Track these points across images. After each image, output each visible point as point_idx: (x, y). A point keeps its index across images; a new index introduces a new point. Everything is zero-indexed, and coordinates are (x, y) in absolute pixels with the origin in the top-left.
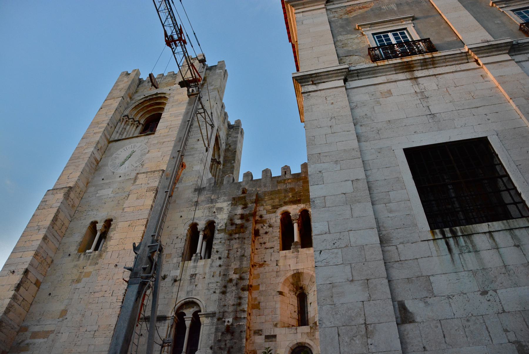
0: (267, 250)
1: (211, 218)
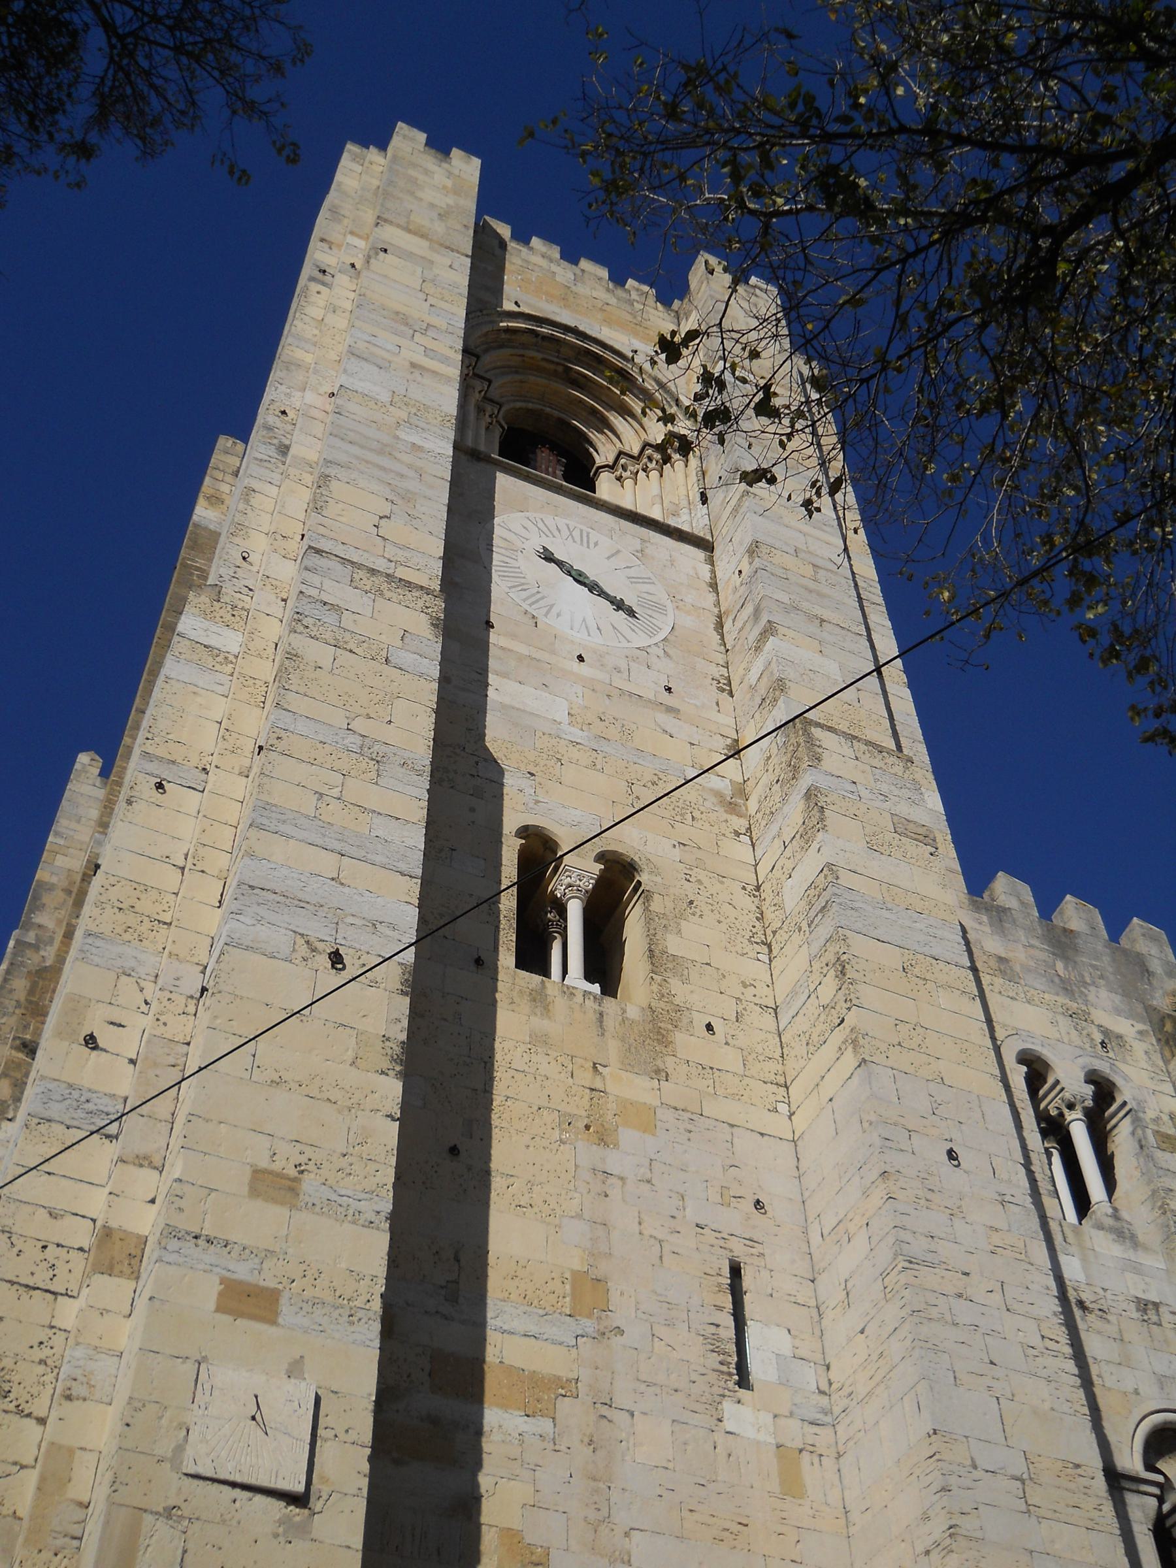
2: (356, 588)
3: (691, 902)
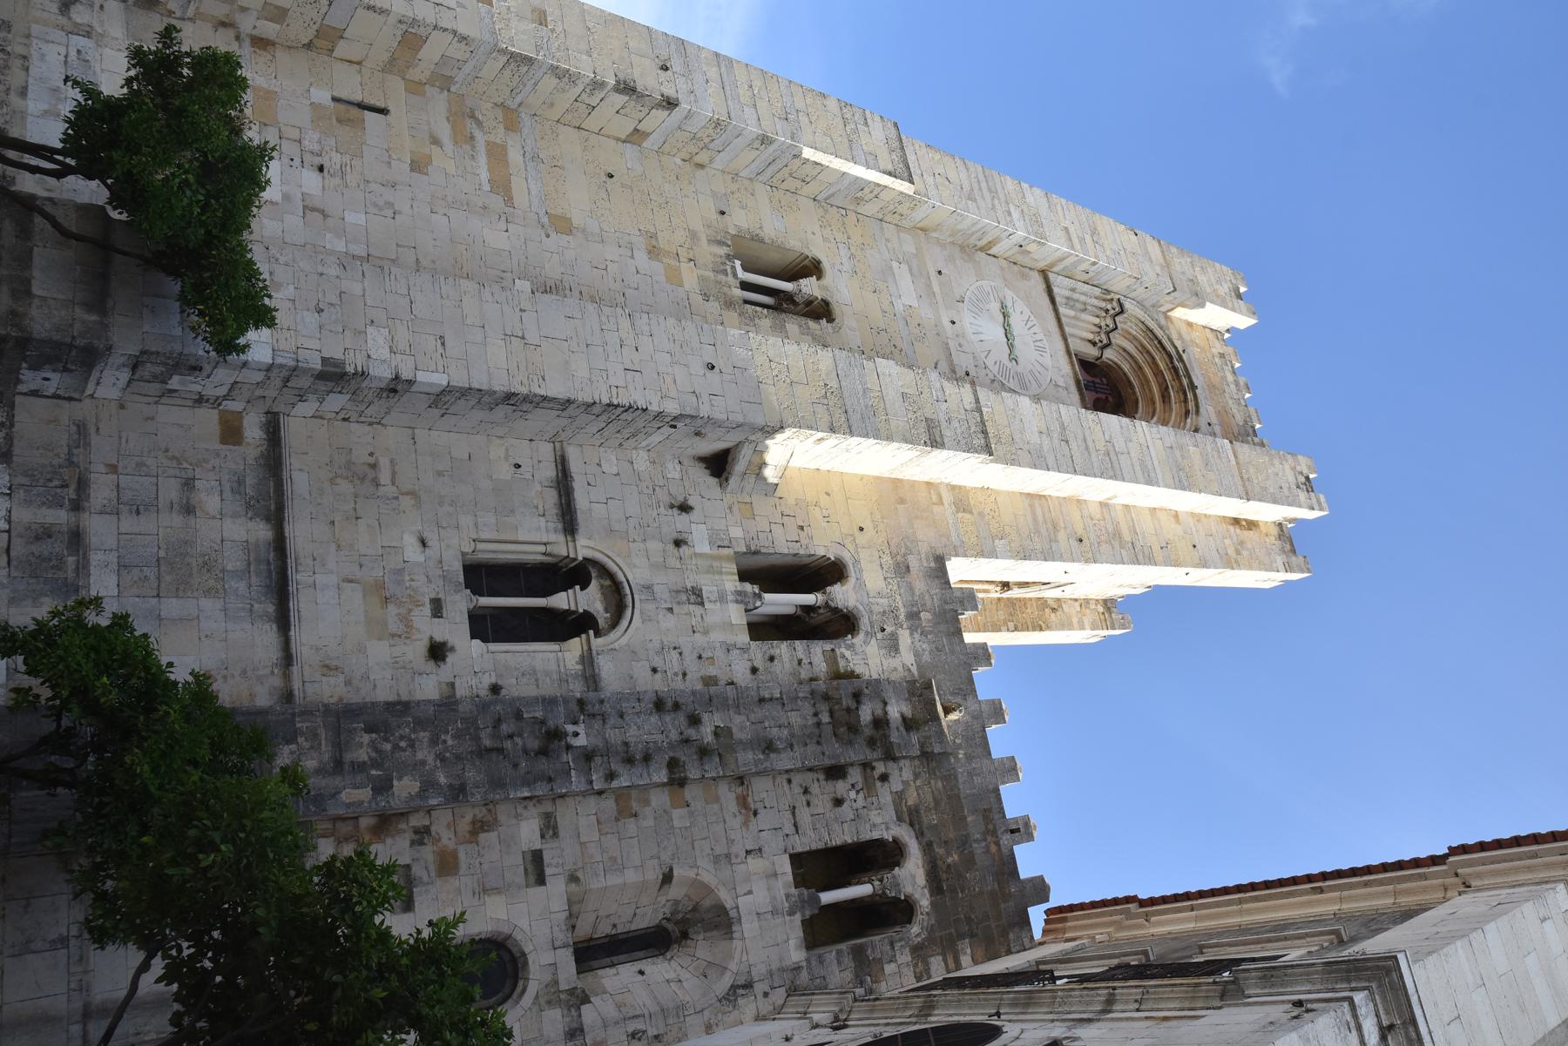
0: (788, 815)
1: (864, 623)
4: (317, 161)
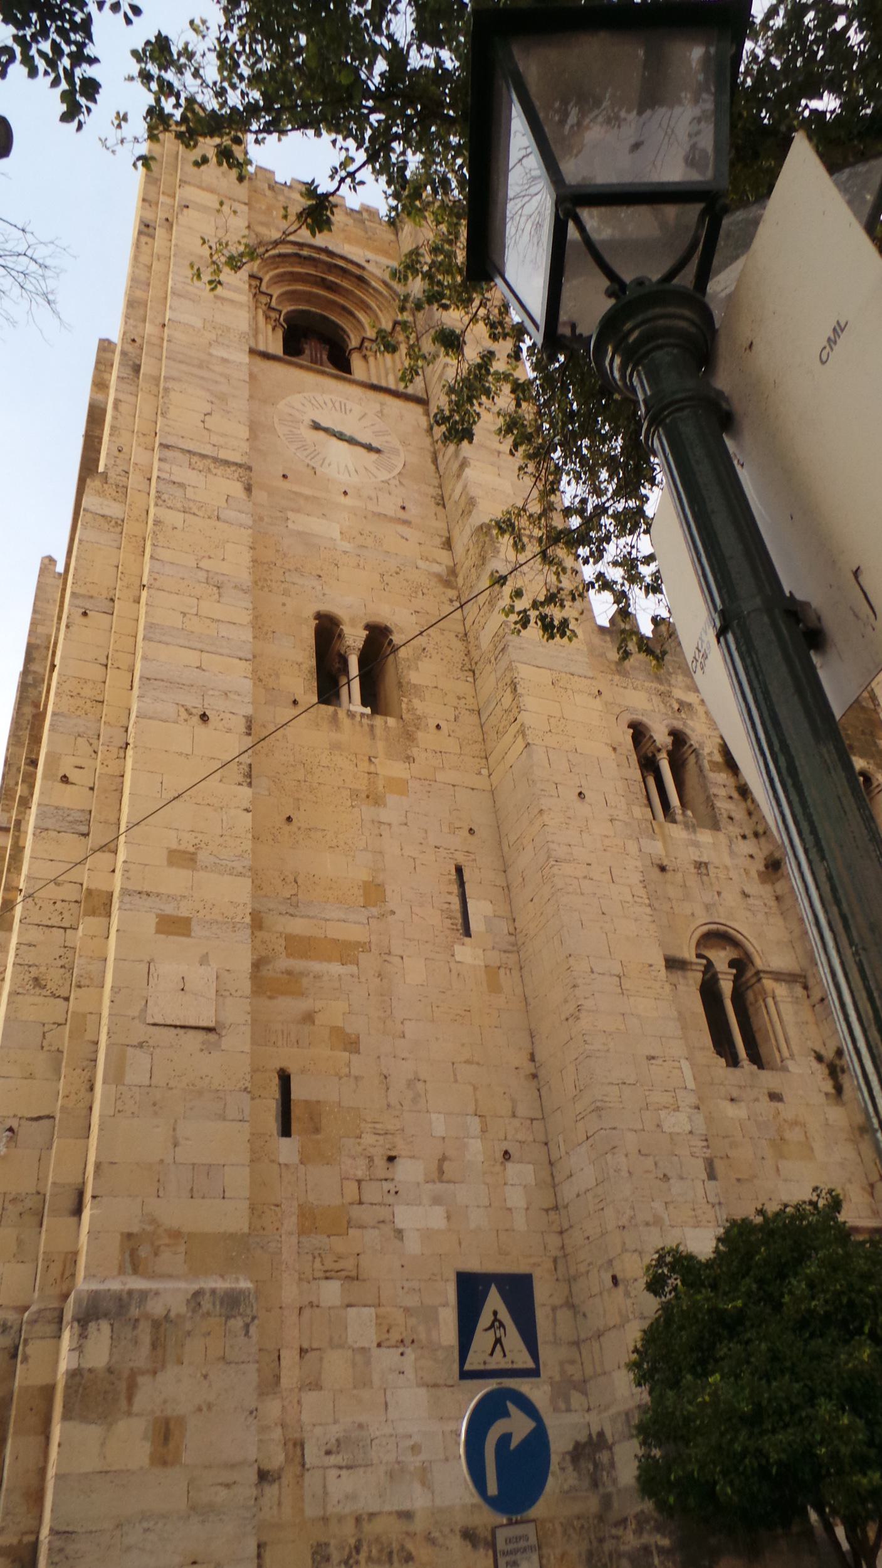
2: (194, 469)
3: (424, 649)
4: (380, 1162)
